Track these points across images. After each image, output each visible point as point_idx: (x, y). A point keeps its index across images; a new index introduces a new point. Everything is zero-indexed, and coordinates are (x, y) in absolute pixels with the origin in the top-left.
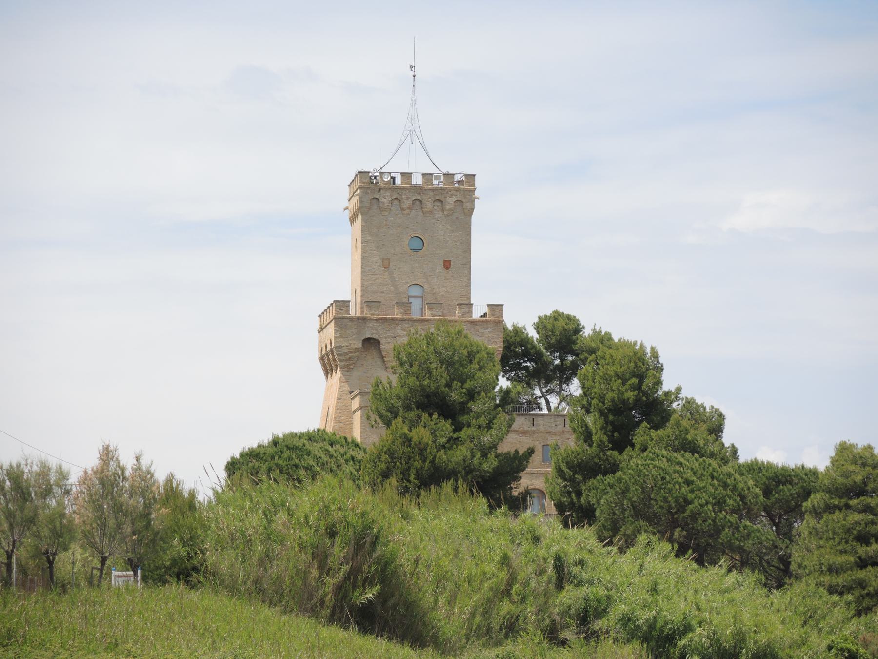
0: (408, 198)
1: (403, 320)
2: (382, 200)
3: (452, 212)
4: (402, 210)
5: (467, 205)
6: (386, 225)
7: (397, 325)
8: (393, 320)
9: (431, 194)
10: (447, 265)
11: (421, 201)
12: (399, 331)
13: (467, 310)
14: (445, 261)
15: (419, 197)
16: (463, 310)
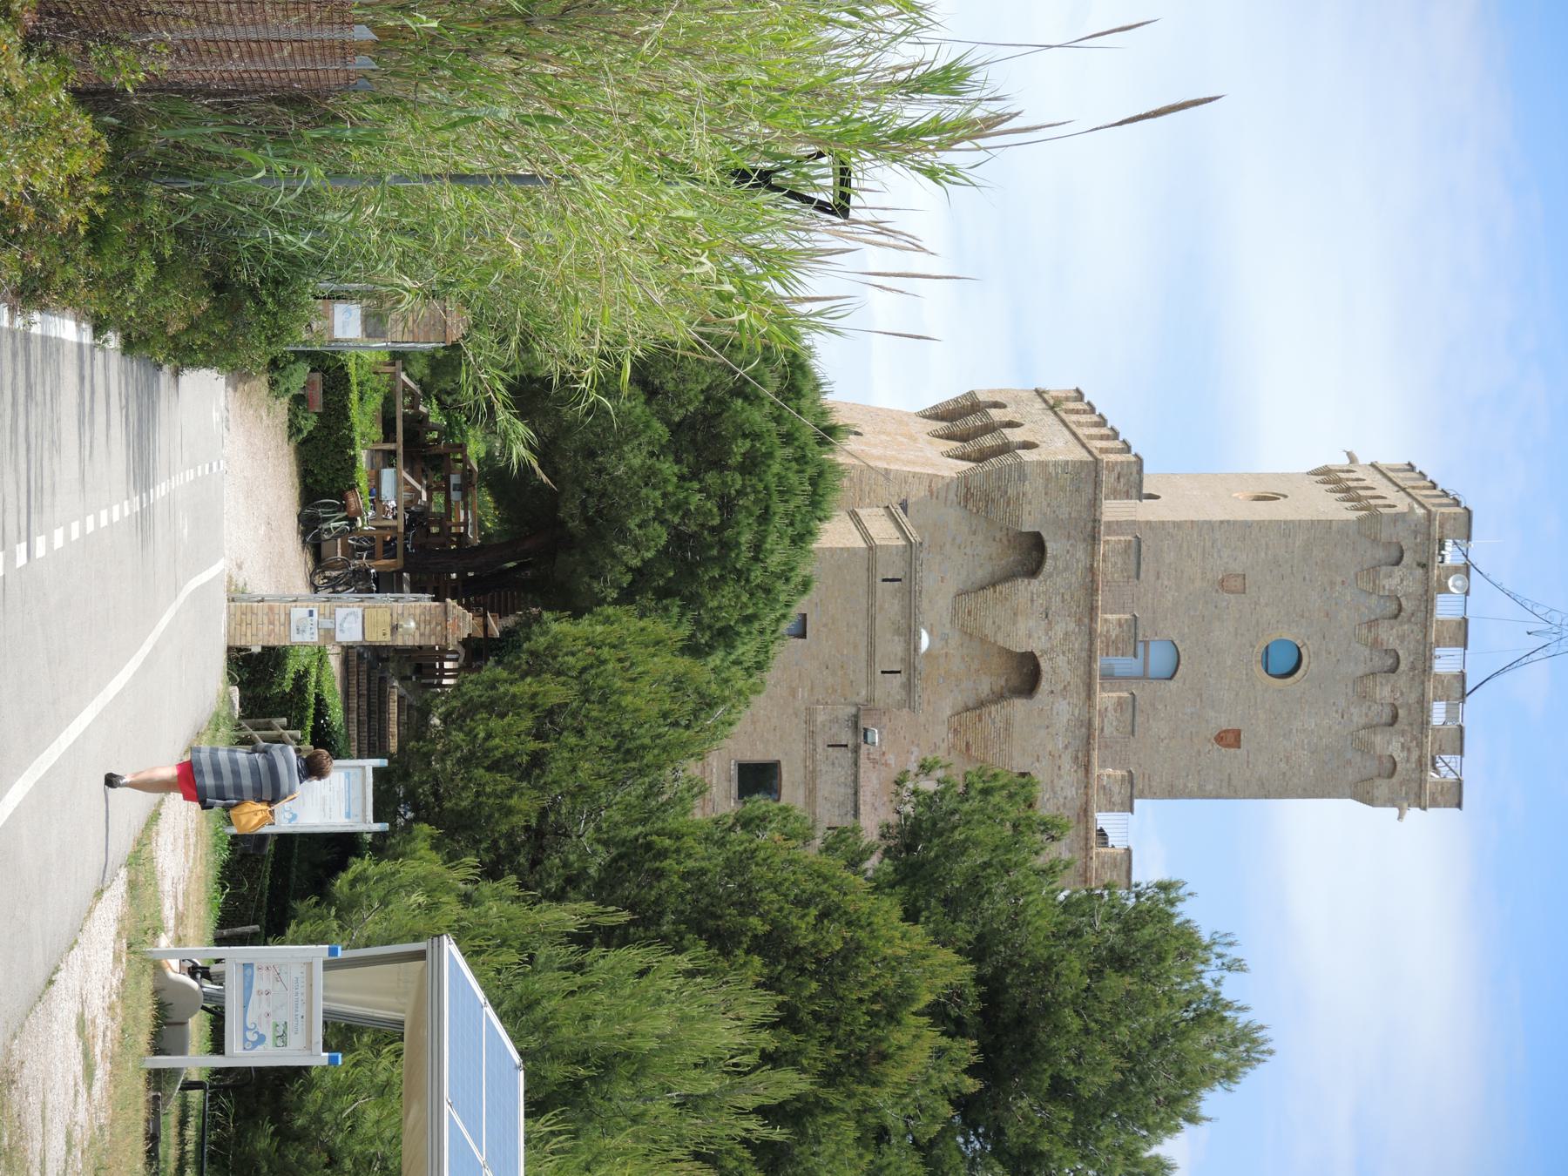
0: (1402, 638)
1: (1091, 633)
2: (1398, 572)
3: (1365, 749)
4: (1372, 624)
5: (1382, 788)
6: (1332, 583)
7: (1079, 622)
8: (1092, 609)
9: (1413, 698)
10: (1229, 738)
11: (1394, 669)
12: (1064, 626)
13: (1117, 799)
14: (1238, 733)
15: (1403, 666)
16: (1116, 789)
